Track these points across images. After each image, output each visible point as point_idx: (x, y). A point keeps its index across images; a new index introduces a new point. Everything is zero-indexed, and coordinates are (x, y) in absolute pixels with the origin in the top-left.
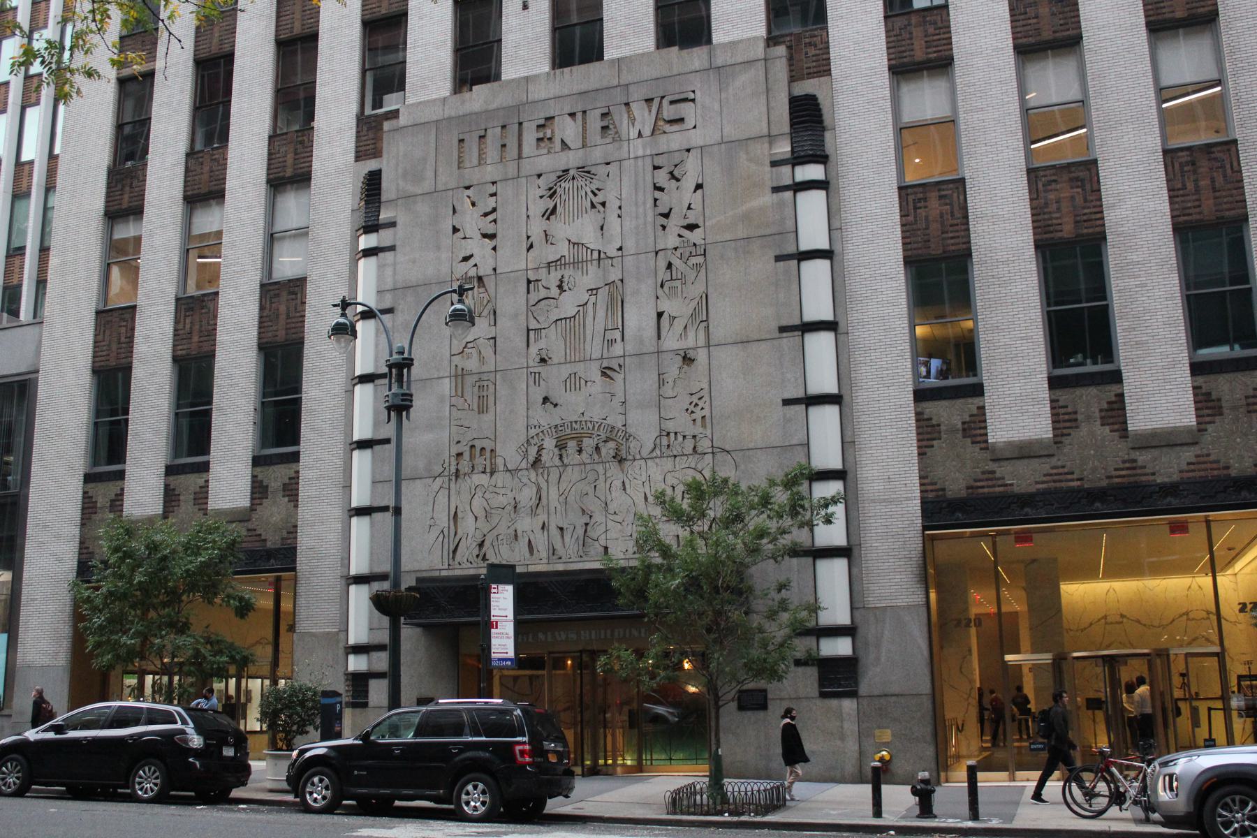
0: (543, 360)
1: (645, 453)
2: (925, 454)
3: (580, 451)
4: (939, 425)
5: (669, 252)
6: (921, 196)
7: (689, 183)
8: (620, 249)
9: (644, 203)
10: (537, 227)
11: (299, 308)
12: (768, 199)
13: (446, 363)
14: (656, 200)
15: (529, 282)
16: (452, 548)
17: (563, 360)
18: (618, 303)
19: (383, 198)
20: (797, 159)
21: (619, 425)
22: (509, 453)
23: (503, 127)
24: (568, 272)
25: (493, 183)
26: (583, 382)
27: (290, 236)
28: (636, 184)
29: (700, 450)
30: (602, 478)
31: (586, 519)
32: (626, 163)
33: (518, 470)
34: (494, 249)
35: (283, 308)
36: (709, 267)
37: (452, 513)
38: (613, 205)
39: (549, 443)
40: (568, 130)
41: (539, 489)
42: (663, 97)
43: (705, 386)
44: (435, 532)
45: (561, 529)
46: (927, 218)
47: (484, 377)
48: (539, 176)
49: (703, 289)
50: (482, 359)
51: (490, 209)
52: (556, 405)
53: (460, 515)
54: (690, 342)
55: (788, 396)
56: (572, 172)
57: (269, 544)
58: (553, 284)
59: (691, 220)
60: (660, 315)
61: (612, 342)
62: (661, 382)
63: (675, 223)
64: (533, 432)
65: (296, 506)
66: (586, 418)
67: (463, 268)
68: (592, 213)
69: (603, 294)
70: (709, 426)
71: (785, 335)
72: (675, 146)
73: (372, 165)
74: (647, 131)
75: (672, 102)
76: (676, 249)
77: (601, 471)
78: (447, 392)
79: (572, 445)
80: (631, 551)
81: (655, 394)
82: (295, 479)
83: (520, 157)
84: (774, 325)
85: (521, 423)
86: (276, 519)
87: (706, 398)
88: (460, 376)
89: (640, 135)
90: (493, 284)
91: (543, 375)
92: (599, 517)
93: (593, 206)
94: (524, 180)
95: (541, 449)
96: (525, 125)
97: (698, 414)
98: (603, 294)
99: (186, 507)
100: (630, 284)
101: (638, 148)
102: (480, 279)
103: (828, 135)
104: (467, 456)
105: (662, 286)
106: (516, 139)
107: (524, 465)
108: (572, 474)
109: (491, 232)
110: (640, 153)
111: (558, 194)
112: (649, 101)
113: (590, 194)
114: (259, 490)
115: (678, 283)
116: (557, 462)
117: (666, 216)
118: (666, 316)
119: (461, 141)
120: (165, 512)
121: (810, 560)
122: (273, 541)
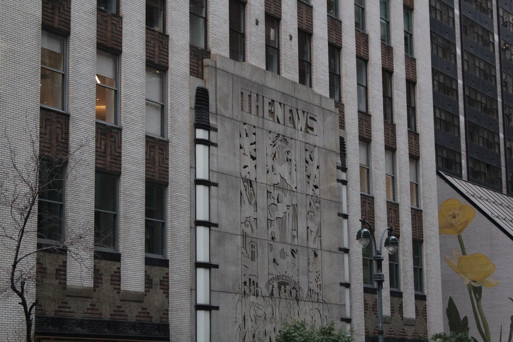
3: (285, 292)
7: (315, 163)
8: (296, 188)
10: (270, 162)
11: (165, 162)
12: (335, 184)
13: (239, 228)
15: (268, 192)
16: (243, 336)
21: (297, 281)
23: (257, 95)
25: (254, 127)
27: (152, 105)
29: (319, 300)
30: (292, 308)
35: (157, 158)
38: (293, 161)
39: (276, 285)
41: (273, 309)
43: (320, 269)
44: (237, 327)
47: (254, 240)
48: (270, 132)
52: (277, 264)
53: (246, 318)
56: (281, 137)
57: (153, 320)
58: (276, 198)
59: (316, 184)
60: (308, 228)
61: (294, 237)
62: (309, 263)
64: (271, 277)
65: (168, 297)
67: (244, 172)
68: (287, 163)
71: (340, 252)
73: (199, 83)
74: (303, 129)
76: (312, 196)
78: (240, 244)
79: (283, 287)
82: (166, 278)
84: (337, 246)
85: (266, 272)
87: (321, 276)
88: (244, 236)
89: (301, 130)
93: (287, 161)
95: (273, 287)
99: (106, 286)
101: (300, 135)
102: (250, 181)
106: (262, 104)
107: (267, 295)
108: (283, 303)
109: (254, 156)
112: (304, 112)
114: (149, 281)
115: (312, 214)
119: (242, 93)
120: (95, 286)
122: (156, 319)
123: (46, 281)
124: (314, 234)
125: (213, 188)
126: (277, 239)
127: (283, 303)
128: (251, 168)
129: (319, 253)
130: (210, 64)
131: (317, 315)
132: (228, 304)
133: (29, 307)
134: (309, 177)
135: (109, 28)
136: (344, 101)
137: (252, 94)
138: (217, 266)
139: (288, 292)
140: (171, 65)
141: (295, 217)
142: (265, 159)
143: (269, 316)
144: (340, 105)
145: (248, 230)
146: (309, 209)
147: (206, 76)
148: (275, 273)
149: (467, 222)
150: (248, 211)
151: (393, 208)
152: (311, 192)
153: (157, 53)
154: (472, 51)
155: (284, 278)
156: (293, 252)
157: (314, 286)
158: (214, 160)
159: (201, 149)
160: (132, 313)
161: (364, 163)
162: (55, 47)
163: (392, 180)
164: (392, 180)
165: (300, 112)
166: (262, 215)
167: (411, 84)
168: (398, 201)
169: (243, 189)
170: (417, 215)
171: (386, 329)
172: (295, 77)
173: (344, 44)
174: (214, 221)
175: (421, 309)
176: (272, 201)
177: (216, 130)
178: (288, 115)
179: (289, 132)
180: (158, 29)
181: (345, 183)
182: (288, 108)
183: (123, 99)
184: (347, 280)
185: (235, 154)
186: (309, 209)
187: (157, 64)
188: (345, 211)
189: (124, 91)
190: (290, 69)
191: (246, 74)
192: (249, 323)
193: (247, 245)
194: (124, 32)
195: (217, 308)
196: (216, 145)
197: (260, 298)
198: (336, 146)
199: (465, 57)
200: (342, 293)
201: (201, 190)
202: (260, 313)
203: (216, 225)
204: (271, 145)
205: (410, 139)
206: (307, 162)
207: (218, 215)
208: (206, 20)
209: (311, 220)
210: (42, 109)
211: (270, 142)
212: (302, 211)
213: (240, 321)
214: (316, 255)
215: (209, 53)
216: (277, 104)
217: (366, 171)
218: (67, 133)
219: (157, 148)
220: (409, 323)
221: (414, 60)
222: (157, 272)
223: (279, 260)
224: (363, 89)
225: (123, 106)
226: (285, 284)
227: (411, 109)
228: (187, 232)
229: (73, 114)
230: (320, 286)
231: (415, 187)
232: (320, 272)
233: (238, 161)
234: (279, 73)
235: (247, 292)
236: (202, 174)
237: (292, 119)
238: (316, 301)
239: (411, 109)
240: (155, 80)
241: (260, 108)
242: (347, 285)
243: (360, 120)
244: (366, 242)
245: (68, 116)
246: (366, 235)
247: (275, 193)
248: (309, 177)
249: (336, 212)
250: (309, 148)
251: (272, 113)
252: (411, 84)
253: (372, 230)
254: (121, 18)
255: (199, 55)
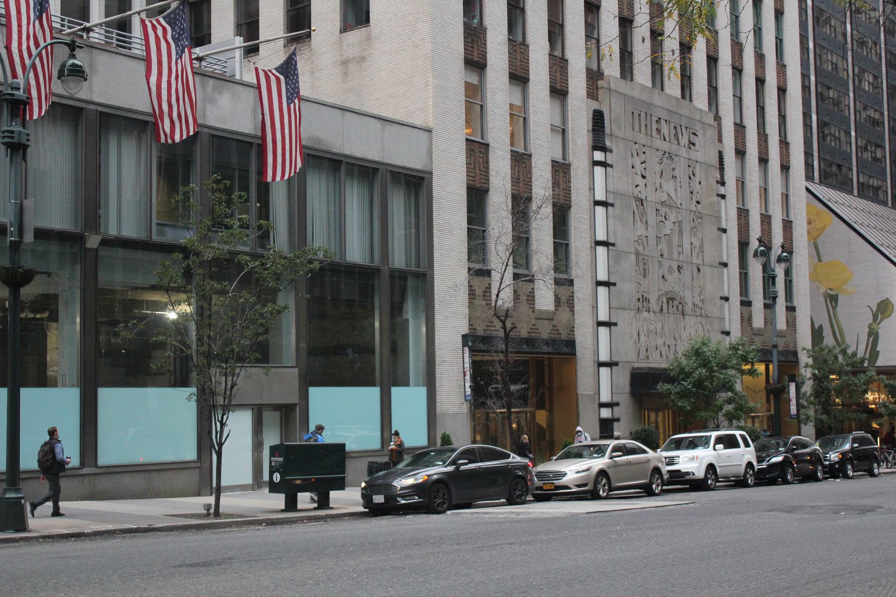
10: (658, 180)
12: (716, 199)
39: (665, 301)
59: (698, 199)
62: (693, 279)
64: (660, 293)
65: (573, 314)
69: (677, 225)
73: (595, 105)
82: (572, 296)
85: (656, 289)
86: (564, 321)
88: (637, 254)
101: (683, 152)
107: (658, 310)
114: (558, 301)
122: (564, 336)
123: (476, 302)
124: (697, 249)
125: (610, 208)
126: (665, 256)
127: (671, 317)
128: (642, 187)
129: (701, 268)
130: (605, 85)
131: (701, 329)
132: (624, 319)
133: (508, 329)
134: (692, 193)
135: (518, 57)
136: (721, 113)
137: (642, 114)
138: (614, 284)
140: (571, 90)
141: (681, 233)
142: (653, 179)
143: (659, 330)
144: (717, 118)
145: (640, 248)
146: (692, 225)
147: (600, 98)
148: (664, 289)
149: (824, 228)
150: (640, 230)
151: (766, 219)
152: (694, 209)
153: (558, 79)
154: (824, 44)
156: (679, 268)
157: (697, 301)
158: (610, 180)
159: (598, 170)
160: (545, 332)
161: (739, 175)
162: (474, 79)
163: (765, 191)
164: (765, 191)
165: (683, 128)
166: (652, 233)
167: (782, 91)
168: (771, 212)
169: (635, 208)
170: (788, 225)
171: (781, 343)
172: (678, 93)
173: (720, 55)
174: (611, 241)
175: (791, 320)
177: (611, 151)
178: (673, 132)
179: (674, 148)
180: (558, 53)
181: (723, 197)
182: (672, 125)
183: (532, 126)
184: (726, 294)
185: (627, 174)
186: (692, 225)
187: (559, 92)
188: (724, 226)
189: (532, 118)
190: (673, 87)
191: (636, 94)
192: (643, 338)
194: (531, 59)
195: (615, 324)
196: (611, 166)
197: (652, 313)
198: (715, 161)
199: (818, 51)
200: (722, 307)
201: (600, 210)
202: (652, 327)
203: (613, 245)
205: (781, 148)
207: (615, 236)
208: (598, 41)
209: (695, 235)
210: (467, 140)
211: (658, 160)
212: (686, 227)
213: (636, 337)
214: (699, 270)
215: (602, 74)
216: (663, 122)
217: (741, 184)
218: (487, 162)
219: (561, 170)
220: (781, 334)
221: (784, 66)
222: (564, 291)
223: (667, 277)
224: (737, 99)
225: (532, 133)
226: (673, 299)
227: (782, 118)
228: (588, 252)
229: (492, 144)
230: (702, 301)
231: (786, 197)
233: (630, 181)
234: (662, 89)
235: (641, 308)
236: (600, 196)
237: (676, 135)
239: (782, 118)
240: (557, 104)
241: (649, 126)
242: (726, 299)
243: (736, 132)
244: (763, 260)
245: (487, 145)
246: (763, 254)
247: (663, 211)
248: (692, 193)
250: (691, 164)
251: (658, 130)
252: (782, 91)
253: (769, 248)
254: (528, 46)
255: (594, 76)
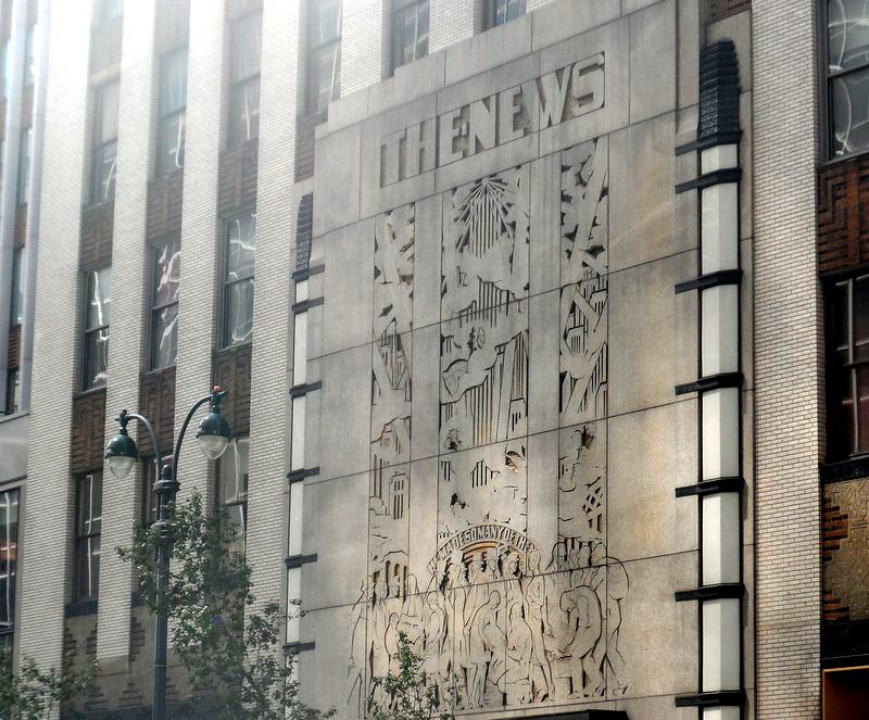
0: (453, 446)
1: (543, 571)
2: (830, 559)
4: (846, 517)
5: (573, 288)
6: (840, 180)
7: (594, 189)
9: (552, 219)
13: (367, 455)
14: (563, 215)
15: (442, 339)
17: (471, 445)
18: (523, 363)
19: (316, 232)
20: (703, 142)
21: (520, 530)
22: (421, 574)
24: (478, 323)
26: (489, 473)
28: (545, 195)
29: (594, 560)
30: (503, 600)
31: (487, 657)
32: (536, 162)
33: (428, 593)
34: (411, 296)
36: (611, 306)
37: (369, 651)
38: (521, 227)
39: (456, 557)
40: (481, 123)
42: (573, 65)
43: (602, 473)
45: (465, 669)
46: (846, 210)
48: (455, 190)
49: (604, 339)
50: (398, 448)
51: (407, 242)
53: (375, 654)
54: (589, 415)
55: (682, 483)
59: (596, 242)
60: (562, 377)
61: (515, 418)
62: (561, 471)
63: (581, 243)
64: (442, 541)
66: (491, 522)
70: (603, 527)
71: (682, 397)
72: (583, 135)
74: (556, 119)
75: (582, 72)
76: (579, 283)
77: (503, 593)
78: (367, 493)
80: (527, 700)
81: (555, 486)
83: (437, 166)
87: (602, 491)
89: (550, 124)
90: (409, 343)
91: (452, 465)
92: (499, 655)
94: (440, 196)
96: (442, 118)
97: (593, 515)
98: (511, 348)
100: (536, 337)
103: (744, 100)
104: (382, 577)
105: (565, 337)
108: (478, 596)
110: (549, 149)
111: (471, 216)
113: (500, 211)
116: (464, 583)
117: (571, 236)
118: (568, 378)
120: (130, 656)
121: (695, 710)
139: (492, 565)
155: (481, 533)
176: (454, 354)
193: (385, 487)
204: (456, 220)
206: (565, 198)
211: (454, 213)
232: (601, 483)
235: (381, 593)
238: (586, 565)
249: (672, 282)
